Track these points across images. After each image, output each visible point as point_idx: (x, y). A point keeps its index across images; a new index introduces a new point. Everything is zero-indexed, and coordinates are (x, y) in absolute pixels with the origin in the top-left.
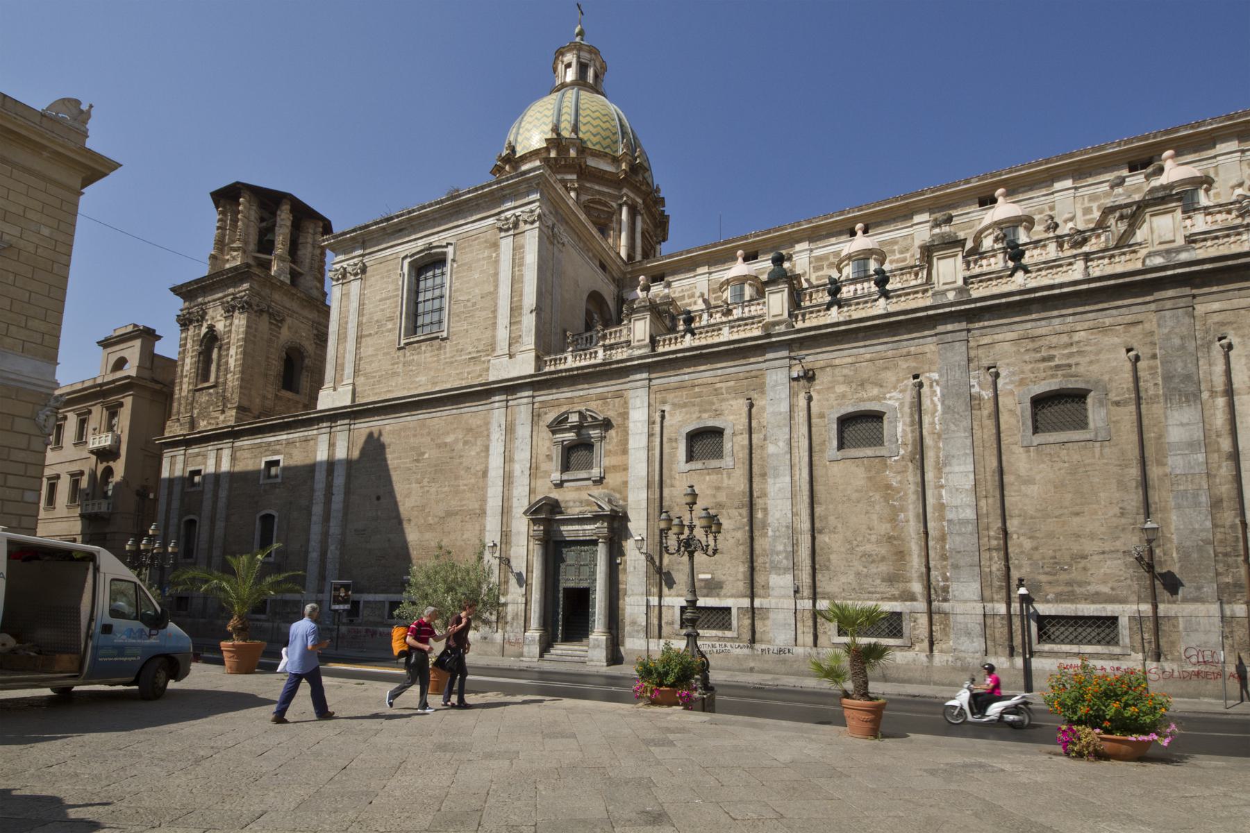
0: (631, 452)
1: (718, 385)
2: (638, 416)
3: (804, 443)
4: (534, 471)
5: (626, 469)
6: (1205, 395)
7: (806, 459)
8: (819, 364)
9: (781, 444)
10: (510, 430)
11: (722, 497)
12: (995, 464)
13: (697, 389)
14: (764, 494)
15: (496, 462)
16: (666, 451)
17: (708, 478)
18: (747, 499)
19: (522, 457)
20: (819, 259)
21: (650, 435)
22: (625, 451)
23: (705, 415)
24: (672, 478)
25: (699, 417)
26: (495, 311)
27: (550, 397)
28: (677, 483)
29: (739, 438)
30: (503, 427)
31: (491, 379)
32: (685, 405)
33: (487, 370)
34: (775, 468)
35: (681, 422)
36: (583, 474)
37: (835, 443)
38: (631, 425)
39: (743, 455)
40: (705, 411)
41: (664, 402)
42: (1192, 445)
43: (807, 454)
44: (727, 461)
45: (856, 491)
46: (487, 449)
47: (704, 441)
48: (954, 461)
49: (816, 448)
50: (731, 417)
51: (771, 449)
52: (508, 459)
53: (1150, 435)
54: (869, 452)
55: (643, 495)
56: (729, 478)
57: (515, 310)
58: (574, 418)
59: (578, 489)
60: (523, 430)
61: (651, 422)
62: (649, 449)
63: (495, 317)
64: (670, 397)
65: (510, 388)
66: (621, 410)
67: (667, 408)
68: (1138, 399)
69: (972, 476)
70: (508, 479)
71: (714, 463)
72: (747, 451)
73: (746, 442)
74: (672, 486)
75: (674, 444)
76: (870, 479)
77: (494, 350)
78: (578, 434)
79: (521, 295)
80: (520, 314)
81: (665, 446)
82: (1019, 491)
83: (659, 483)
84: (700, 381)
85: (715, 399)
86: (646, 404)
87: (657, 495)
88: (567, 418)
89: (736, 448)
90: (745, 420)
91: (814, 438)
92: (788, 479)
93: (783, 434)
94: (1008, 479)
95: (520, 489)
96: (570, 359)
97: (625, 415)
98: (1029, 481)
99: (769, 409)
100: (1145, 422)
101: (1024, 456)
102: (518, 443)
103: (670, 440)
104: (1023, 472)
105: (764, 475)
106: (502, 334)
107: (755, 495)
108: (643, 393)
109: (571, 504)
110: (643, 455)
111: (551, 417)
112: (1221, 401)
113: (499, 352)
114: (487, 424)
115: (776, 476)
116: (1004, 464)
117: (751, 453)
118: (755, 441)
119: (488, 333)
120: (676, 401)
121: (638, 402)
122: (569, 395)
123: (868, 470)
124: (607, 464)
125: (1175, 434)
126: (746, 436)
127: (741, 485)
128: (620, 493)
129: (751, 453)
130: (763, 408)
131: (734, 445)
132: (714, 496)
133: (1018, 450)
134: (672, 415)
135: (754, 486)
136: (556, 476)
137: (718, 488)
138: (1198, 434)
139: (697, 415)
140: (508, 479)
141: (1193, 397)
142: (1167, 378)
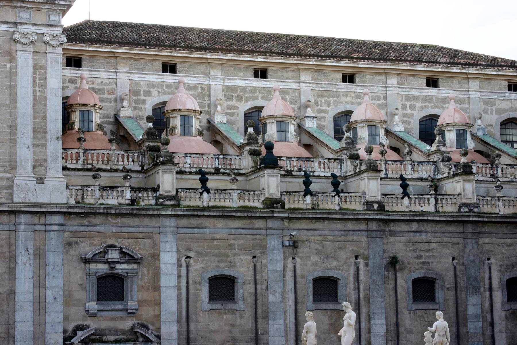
0: (163, 289)
1: (232, 242)
2: (168, 258)
3: (291, 296)
4: (68, 300)
5: (158, 303)
6: (482, 289)
7: (293, 307)
8: (304, 238)
9: (278, 295)
10: (40, 254)
11: (236, 333)
12: (395, 320)
13: (215, 243)
14: (266, 332)
15: (24, 286)
16: (192, 291)
17: (225, 316)
18: (254, 335)
19: (55, 284)
20: (229, 89)
21: (179, 277)
22: (157, 288)
23: (222, 265)
24: (196, 314)
25: (218, 266)
26: (13, 127)
27: (82, 228)
28: (201, 319)
29: (248, 286)
30: (31, 251)
31: (16, 200)
32: (206, 255)
33: (11, 187)
34: (274, 313)
35: (203, 268)
36: (118, 306)
37: (311, 298)
38: (162, 266)
39: (250, 300)
40: (222, 261)
41: (189, 249)
42: (477, 317)
43: (293, 304)
44: (241, 305)
45: (324, 333)
46: (12, 272)
47: (222, 288)
48: (376, 317)
49: (300, 300)
50: (242, 270)
51: (271, 298)
52: (40, 285)
53: (461, 309)
54: (331, 306)
55: (175, 328)
56: (241, 317)
57: (39, 131)
58: (114, 255)
59: (112, 319)
60: (55, 258)
61: (179, 266)
62: (179, 288)
63: (16, 134)
64: (194, 245)
65: (40, 212)
66: (151, 251)
67: (192, 254)
68: (456, 288)
69: (385, 327)
70: (40, 307)
71: (230, 306)
72: (254, 298)
73: (252, 291)
74: (197, 321)
75: (198, 287)
76: (331, 325)
77: (14, 167)
78: (112, 268)
79: (45, 117)
80: (45, 138)
81: (191, 287)
82: (406, 337)
83: (186, 318)
84: (218, 236)
85: (230, 253)
86: (175, 249)
87: (184, 329)
88: (106, 253)
89: (246, 294)
90: (252, 273)
91: (299, 292)
92: (282, 322)
93: (278, 287)
94: (402, 329)
95: (53, 315)
96: (97, 194)
97: (156, 257)
98: (410, 332)
99: (270, 268)
100: (459, 301)
101: (408, 316)
102: (49, 269)
103: (195, 282)
104: (408, 326)
105: (266, 317)
106: (25, 154)
107: (260, 332)
108: (170, 238)
109: (107, 332)
110: (173, 294)
111: (88, 249)
112: (488, 293)
113: (20, 171)
114: (12, 246)
115: (274, 319)
116: (399, 320)
117: (256, 300)
118: (259, 290)
119: (6, 149)
120: (199, 249)
121: (168, 247)
122: (102, 229)
123: (330, 318)
124: (140, 298)
125: (471, 310)
126: (252, 285)
127: (250, 325)
128: (153, 324)
129: (256, 300)
130: (266, 266)
131: (244, 291)
132: (231, 332)
133: (406, 312)
134: (195, 262)
135: (259, 325)
136: (93, 306)
137: (233, 326)
138: (479, 312)
139: (215, 264)
140: (40, 307)
141: (477, 290)
142: (468, 278)
